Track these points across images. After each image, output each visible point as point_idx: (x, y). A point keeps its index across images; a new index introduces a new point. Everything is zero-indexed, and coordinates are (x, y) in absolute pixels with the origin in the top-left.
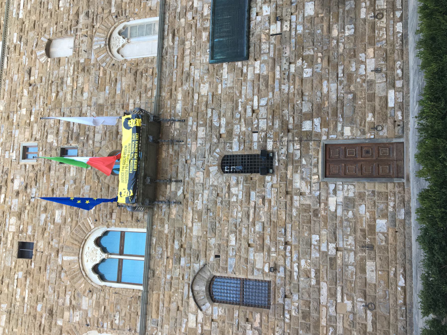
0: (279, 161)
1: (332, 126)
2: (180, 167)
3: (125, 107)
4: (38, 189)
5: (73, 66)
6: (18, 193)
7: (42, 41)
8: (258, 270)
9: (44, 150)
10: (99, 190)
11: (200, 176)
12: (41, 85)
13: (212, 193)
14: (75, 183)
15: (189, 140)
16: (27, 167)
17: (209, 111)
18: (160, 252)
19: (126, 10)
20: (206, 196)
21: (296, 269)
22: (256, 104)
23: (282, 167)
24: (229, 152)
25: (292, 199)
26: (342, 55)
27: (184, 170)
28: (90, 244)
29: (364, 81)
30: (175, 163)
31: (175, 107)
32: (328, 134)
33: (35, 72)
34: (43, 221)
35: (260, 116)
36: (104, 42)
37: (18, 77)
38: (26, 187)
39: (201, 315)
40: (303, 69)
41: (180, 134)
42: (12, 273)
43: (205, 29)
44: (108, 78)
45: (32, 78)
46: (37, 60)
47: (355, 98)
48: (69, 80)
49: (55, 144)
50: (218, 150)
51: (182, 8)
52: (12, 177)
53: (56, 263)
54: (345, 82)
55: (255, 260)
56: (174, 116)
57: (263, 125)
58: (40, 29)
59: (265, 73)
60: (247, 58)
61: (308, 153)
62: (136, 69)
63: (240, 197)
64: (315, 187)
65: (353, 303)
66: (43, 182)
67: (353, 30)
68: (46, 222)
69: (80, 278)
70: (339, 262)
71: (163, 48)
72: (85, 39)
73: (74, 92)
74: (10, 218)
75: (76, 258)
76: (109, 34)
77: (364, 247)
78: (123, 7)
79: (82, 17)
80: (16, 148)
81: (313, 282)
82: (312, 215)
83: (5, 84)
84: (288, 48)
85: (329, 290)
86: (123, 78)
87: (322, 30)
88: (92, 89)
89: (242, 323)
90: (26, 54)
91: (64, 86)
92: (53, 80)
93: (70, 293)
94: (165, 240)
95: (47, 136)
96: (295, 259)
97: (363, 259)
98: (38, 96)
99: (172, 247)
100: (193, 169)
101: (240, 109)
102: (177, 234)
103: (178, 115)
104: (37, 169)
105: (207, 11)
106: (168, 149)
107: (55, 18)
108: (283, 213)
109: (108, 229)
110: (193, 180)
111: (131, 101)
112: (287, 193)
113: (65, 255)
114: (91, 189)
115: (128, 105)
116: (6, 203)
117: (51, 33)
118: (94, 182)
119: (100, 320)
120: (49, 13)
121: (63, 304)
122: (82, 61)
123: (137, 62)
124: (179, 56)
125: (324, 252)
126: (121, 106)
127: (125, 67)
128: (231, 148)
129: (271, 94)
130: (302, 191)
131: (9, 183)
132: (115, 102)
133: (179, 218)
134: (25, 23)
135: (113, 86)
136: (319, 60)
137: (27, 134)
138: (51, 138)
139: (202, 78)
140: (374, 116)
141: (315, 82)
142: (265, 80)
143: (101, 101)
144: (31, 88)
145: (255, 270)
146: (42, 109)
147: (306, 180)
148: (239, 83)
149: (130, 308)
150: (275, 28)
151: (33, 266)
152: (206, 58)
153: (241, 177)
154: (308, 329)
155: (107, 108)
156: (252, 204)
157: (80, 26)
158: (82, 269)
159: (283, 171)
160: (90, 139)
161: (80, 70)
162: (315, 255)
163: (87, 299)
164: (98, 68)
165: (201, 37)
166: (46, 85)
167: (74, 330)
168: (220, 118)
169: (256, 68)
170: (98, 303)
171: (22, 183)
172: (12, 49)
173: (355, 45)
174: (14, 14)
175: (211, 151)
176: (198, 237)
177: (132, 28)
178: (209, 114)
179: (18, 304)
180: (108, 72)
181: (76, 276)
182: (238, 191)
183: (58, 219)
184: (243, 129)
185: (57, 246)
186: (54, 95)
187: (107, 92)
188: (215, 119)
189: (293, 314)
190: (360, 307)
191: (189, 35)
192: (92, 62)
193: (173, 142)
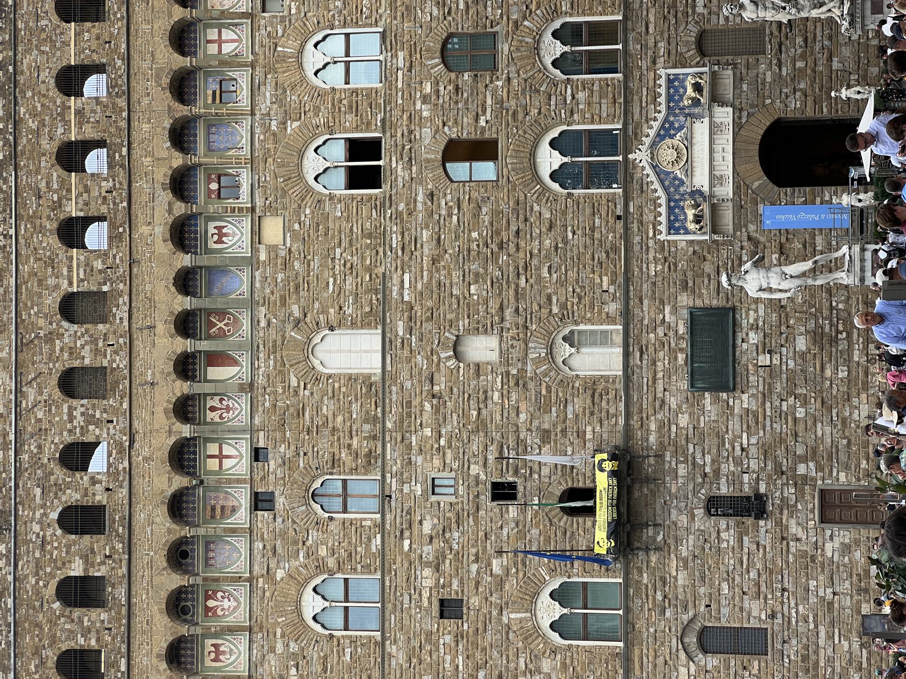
0: (773, 505)
1: (827, 471)
2: (658, 509)
6: (431, 538)
8: (755, 618)
10: (553, 536)
11: (684, 520)
13: (699, 539)
14: (517, 525)
15: (668, 478)
16: (442, 505)
17: (691, 446)
18: (640, 604)
19: (573, 312)
20: (691, 542)
21: (794, 615)
22: (745, 441)
23: (777, 512)
24: (715, 492)
25: (788, 544)
26: (835, 397)
27: (664, 512)
28: (544, 598)
29: (858, 427)
30: (651, 504)
31: (648, 439)
32: (823, 479)
35: (750, 456)
37: (413, 385)
39: (693, 667)
40: (795, 408)
41: (655, 472)
43: (681, 350)
45: (436, 388)
46: (442, 364)
47: (849, 442)
48: (496, 395)
49: (483, 477)
50: (703, 491)
51: (650, 318)
53: (501, 622)
54: (839, 427)
55: (751, 609)
56: (647, 448)
57: (754, 465)
59: (754, 408)
60: (734, 389)
61: (803, 497)
62: (594, 387)
63: (732, 543)
64: (812, 533)
65: (849, 643)
67: (846, 373)
68: (478, 572)
69: (537, 637)
70: (836, 605)
71: (628, 366)
72: (515, 343)
74: (422, 570)
75: (529, 615)
77: (860, 590)
78: (569, 307)
79: (508, 313)
81: (812, 626)
82: (810, 561)
83: (390, 393)
84: (779, 383)
85: (828, 632)
87: (815, 368)
88: (531, 409)
89: (740, 672)
90: (422, 354)
91: (489, 402)
92: (471, 392)
94: (644, 590)
96: (793, 604)
97: (859, 602)
99: (654, 598)
100: (674, 512)
101: (727, 446)
102: (659, 584)
103: (652, 449)
105: (682, 330)
106: (641, 487)
108: (780, 559)
110: (675, 523)
111: (589, 429)
112: (783, 538)
113: (512, 612)
116: (413, 550)
118: (545, 526)
121: (516, 669)
122: (514, 372)
124: (650, 379)
125: (821, 597)
128: (719, 489)
129: (761, 433)
130: (798, 537)
131: (416, 526)
133: (660, 566)
134: (416, 308)
136: (813, 400)
137: (437, 462)
138: (475, 469)
139: (680, 407)
140: (868, 462)
141: (809, 423)
142: (754, 416)
143: (546, 426)
144: (435, 401)
145: (751, 618)
146: (457, 431)
147: (802, 526)
148: (725, 418)
149: (607, 666)
150: (764, 360)
151: (466, 627)
152: (684, 385)
153: (732, 521)
154: (807, 671)
155: (556, 435)
156: (746, 550)
158: (537, 628)
159: (778, 515)
160: (535, 472)
161: (512, 384)
162: (813, 600)
163: (549, 660)
165: (676, 358)
166: (461, 399)
168: (704, 455)
169: (744, 401)
170: (564, 665)
171: (435, 525)
173: (849, 388)
174: (394, 293)
175: (695, 492)
176: (684, 586)
177: (580, 332)
178: (691, 450)
181: (531, 635)
182: (729, 537)
184: (732, 468)
186: (475, 413)
188: (698, 456)
189: (792, 658)
190: (856, 646)
191: (661, 354)
193: (648, 480)
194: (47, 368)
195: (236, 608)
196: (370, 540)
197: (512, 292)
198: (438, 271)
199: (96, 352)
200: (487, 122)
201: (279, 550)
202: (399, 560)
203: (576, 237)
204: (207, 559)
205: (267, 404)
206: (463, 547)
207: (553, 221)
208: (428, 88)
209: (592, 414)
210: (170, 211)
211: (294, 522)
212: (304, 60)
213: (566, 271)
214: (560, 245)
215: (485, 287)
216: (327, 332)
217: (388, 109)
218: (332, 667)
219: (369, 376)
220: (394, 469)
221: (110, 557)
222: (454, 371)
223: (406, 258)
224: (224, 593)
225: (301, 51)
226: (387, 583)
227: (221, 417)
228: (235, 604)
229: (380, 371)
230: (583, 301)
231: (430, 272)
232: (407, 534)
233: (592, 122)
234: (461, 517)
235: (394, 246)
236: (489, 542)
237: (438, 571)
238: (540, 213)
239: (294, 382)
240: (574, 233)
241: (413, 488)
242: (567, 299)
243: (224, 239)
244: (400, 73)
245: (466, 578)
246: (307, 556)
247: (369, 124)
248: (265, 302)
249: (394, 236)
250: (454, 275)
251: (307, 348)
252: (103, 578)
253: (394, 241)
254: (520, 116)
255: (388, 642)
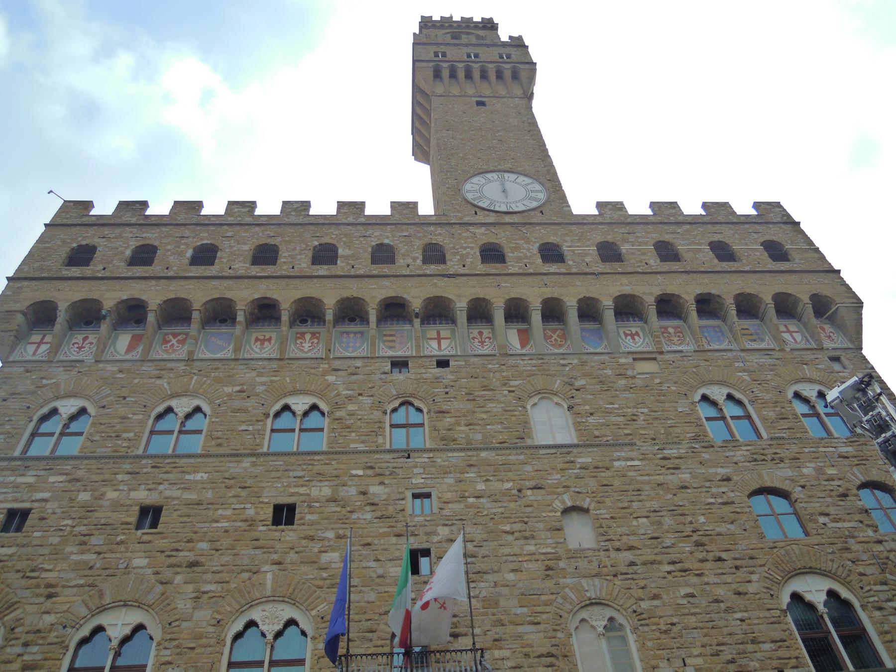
3: (496, 643)
4: (370, 522)
5: (553, 551)
7: (584, 500)
9: (427, 523)
10: (367, 616)
12: (520, 506)
14: (380, 577)
16: (401, 502)
19: (647, 625)
28: (288, 612)
33: (539, 495)
34: (323, 535)
36: (593, 596)
38: (373, 504)
42: (253, 500)
44: (539, 609)
45: (529, 492)
48: (532, 548)
49: (436, 539)
52: (386, 482)
58: (601, 495)
66: (380, 527)
69: (239, 603)
72: (596, 564)
73: (515, 558)
74: (329, 486)
75: (269, 593)
76: (607, 602)
79: (628, 556)
80: (429, 481)
83: (517, 454)
86: (542, 634)
88: (521, 585)
90: (563, 479)
91: (522, 542)
92: (530, 524)
93: (219, 589)
95: (446, 525)
98: (505, 505)
104: (400, 517)
107: (620, 515)
109: (309, 639)
111: (507, 653)
113: (274, 574)
114: (368, 602)
115: (501, 648)
117: (598, 512)
118: (379, 607)
119: (175, 643)
120: (626, 505)
122: (562, 564)
123: (568, 654)
126: (497, 636)
127: (560, 635)
131: (378, 480)
132: (503, 625)
135: (528, 619)
137: (448, 496)
143: (503, 603)
144: (515, 492)
146: (485, 513)
155: (494, 615)
157: (613, 554)
161: (547, 563)
163: (209, 618)
164: (553, 591)
167: (166, 602)
172: (568, 458)
177: (624, 638)
179: (211, 513)
180: (548, 609)
183: (325, 558)
185: (288, 560)
186: (507, 528)
187: (519, 611)
192: (561, 581)
194: (501, 237)
195: (303, 351)
196: (363, 442)
197: (651, 558)
198: (653, 489)
199: (518, 259)
200: (824, 524)
201: (354, 377)
202: (342, 466)
203: (739, 622)
204: (348, 333)
205: (490, 366)
206: (354, 523)
207: (747, 597)
208: (831, 471)
209: (527, 655)
210: (644, 293)
211: (380, 387)
212: (804, 384)
213: (694, 614)
214: (722, 605)
215: (649, 532)
216: (566, 407)
217: (796, 441)
218: (235, 416)
219: (530, 437)
220: (439, 460)
221: (353, 267)
222: (550, 508)
223: (657, 462)
224: (317, 343)
225: (811, 381)
226: (316, 457)
227: (473, 338)
228: (306, 350)
229: (536, 443)
230: (663, 636)
231: (649, 483)
232: (370, 472)
233: (881, 633)
234: (388, 520)
235: (665, 452)
236: (360, 548)
237: (328, 501)
238: (749, 582)
239: (512, 383)
240: (742, 620)
241: (419, 476)
242: (661, 617)
243: (629, 337)
244: (833, 449)
245: (318, 527)
246: (349, 398)
247: (773, 428)
248: (583, 363)
249: (675, 451)
250: (653, 503)
251: (545, 393)
252: (336, 264)
253: (670, 452)
254: (850, 556)
255: (254, 459)
